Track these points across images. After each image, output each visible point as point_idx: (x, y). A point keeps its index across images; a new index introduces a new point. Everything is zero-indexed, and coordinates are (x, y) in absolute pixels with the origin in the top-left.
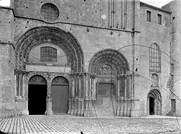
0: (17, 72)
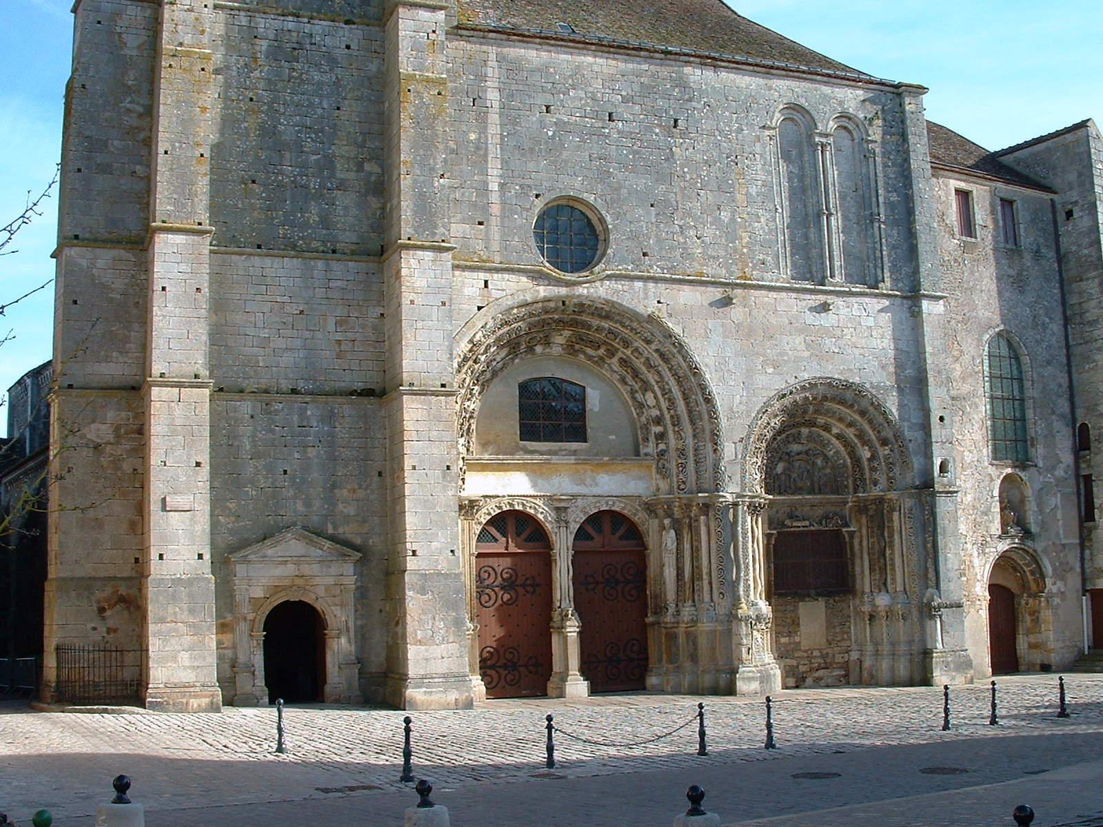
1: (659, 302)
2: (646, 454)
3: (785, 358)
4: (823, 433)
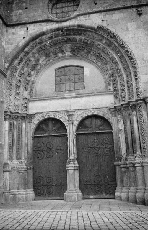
0: (9, 115)
1: (103, 21)
2: (109, 89)
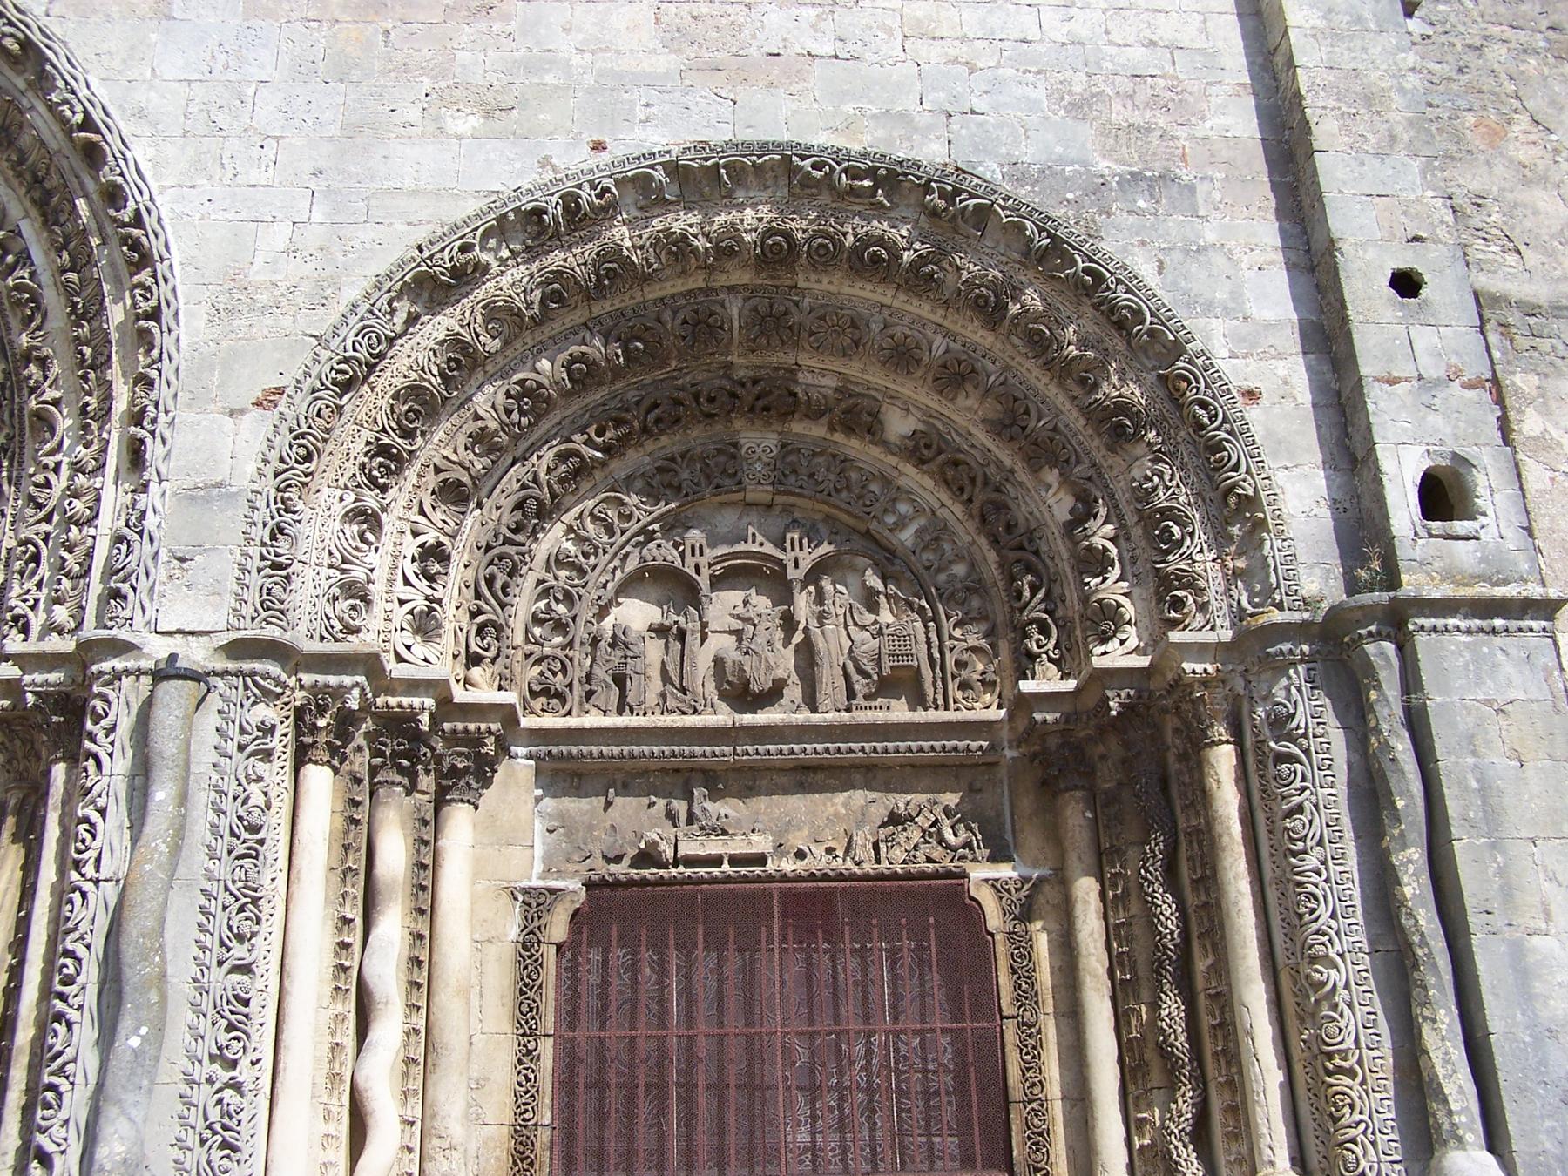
3: (549, 79)
4: (853, 446)
